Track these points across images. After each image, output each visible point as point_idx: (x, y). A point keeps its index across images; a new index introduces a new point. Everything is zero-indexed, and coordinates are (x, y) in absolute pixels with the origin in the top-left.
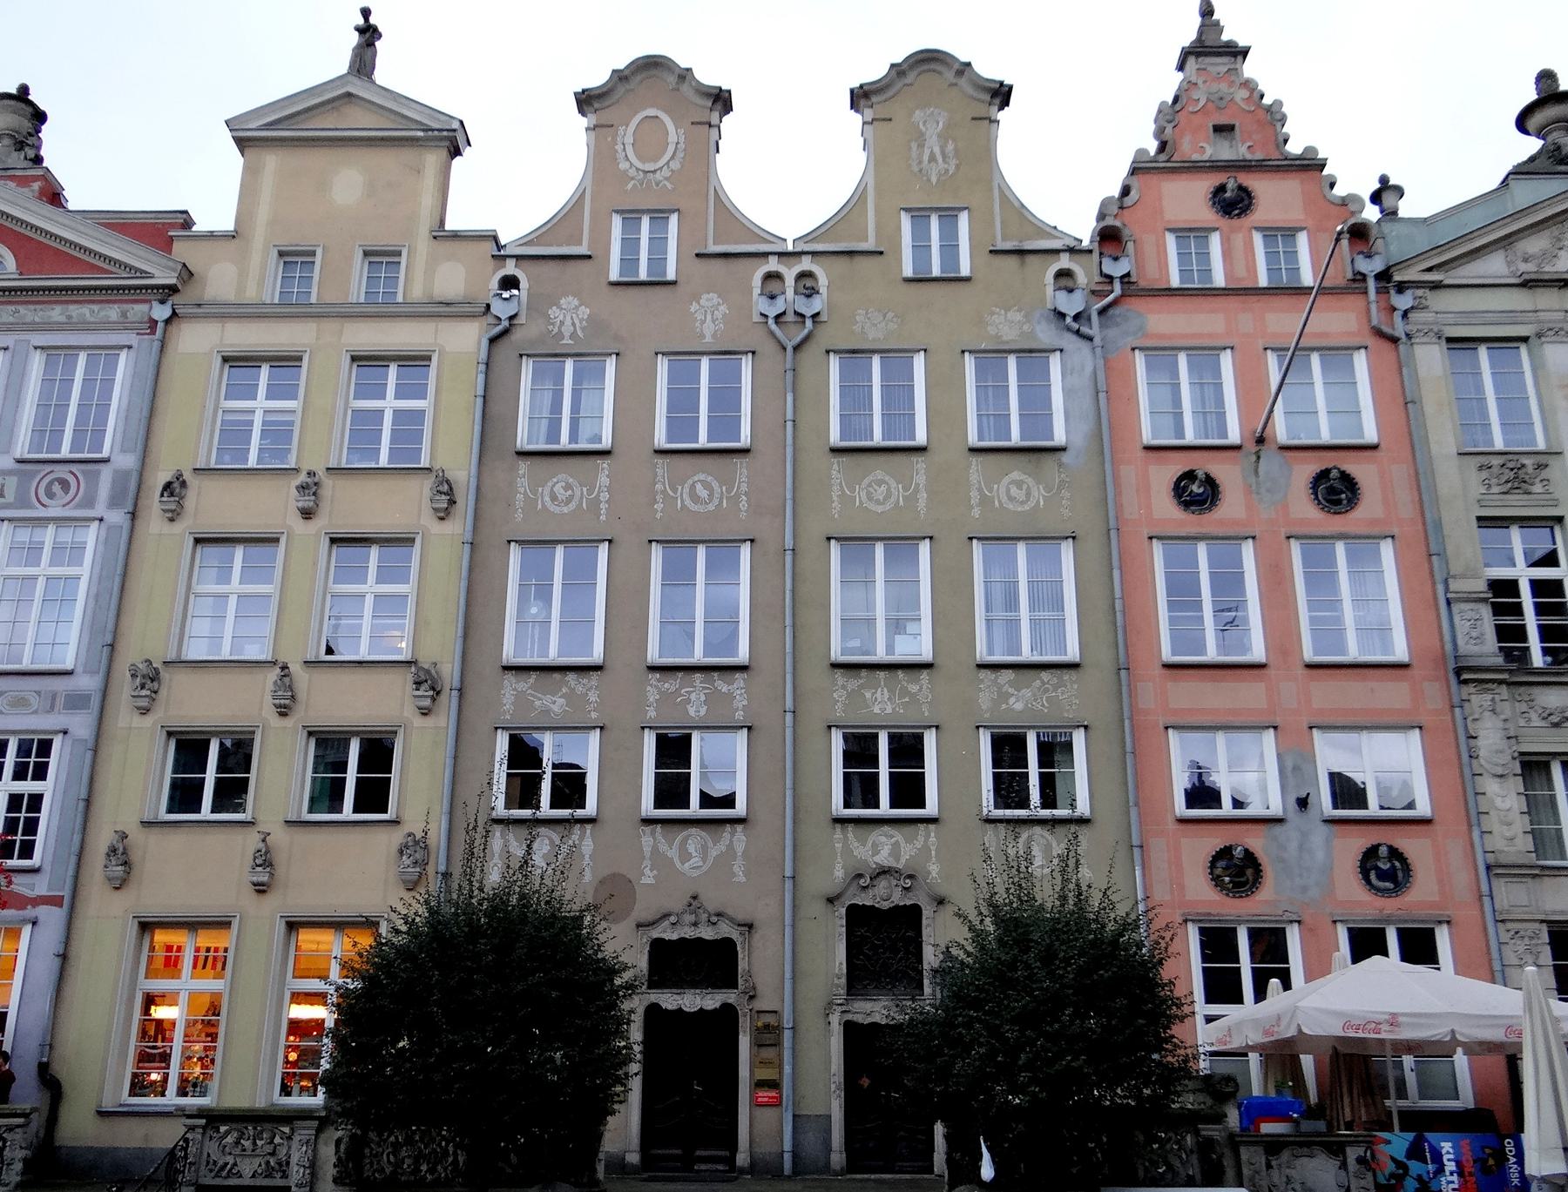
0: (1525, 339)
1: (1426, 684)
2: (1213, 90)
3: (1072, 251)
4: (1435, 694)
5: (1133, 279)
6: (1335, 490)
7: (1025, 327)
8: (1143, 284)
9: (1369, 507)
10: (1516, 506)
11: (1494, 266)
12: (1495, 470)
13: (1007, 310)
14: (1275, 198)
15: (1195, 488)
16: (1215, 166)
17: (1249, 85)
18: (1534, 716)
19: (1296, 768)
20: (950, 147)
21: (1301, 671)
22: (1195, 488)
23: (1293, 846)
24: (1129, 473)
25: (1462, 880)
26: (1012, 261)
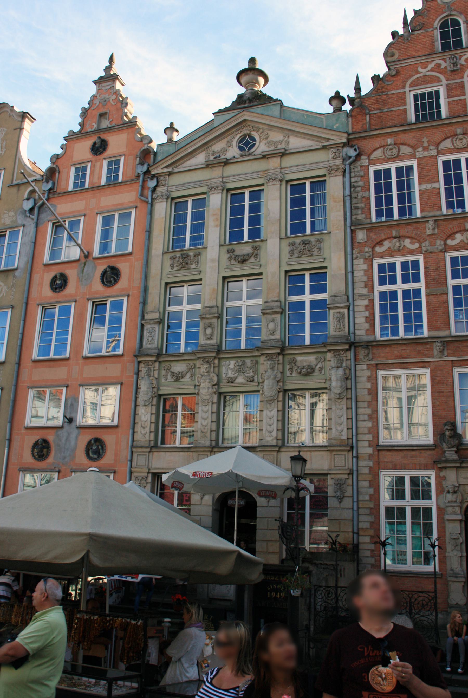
0: (205, 193)
1: (128, 364)
2: (103, 98)
3: (35, 181)
4: (131, 368)
5: (55, 190)
6: (111, 276)
7: (14, 218)
8: (59, 191)
9: (123, 283)
10: (184, 275)
11: (200, 159)
12: (177, 259)
13: (9, 211)
14: (117, 143)
15: (59, 282)
16: (94, 132)
17: (117, 93)
18: (169, 377)
19: (72, 405)
20: (4, 144)
21: (81, 361)
22: (59, 282)
23: (64, 439)
24: (36, 277)
25: (126, 453)
26: (14, 190)
